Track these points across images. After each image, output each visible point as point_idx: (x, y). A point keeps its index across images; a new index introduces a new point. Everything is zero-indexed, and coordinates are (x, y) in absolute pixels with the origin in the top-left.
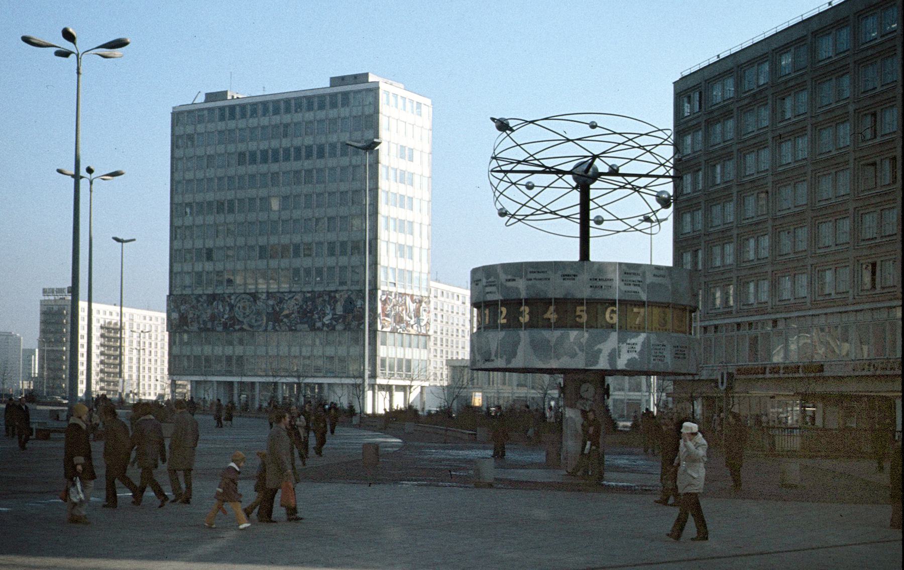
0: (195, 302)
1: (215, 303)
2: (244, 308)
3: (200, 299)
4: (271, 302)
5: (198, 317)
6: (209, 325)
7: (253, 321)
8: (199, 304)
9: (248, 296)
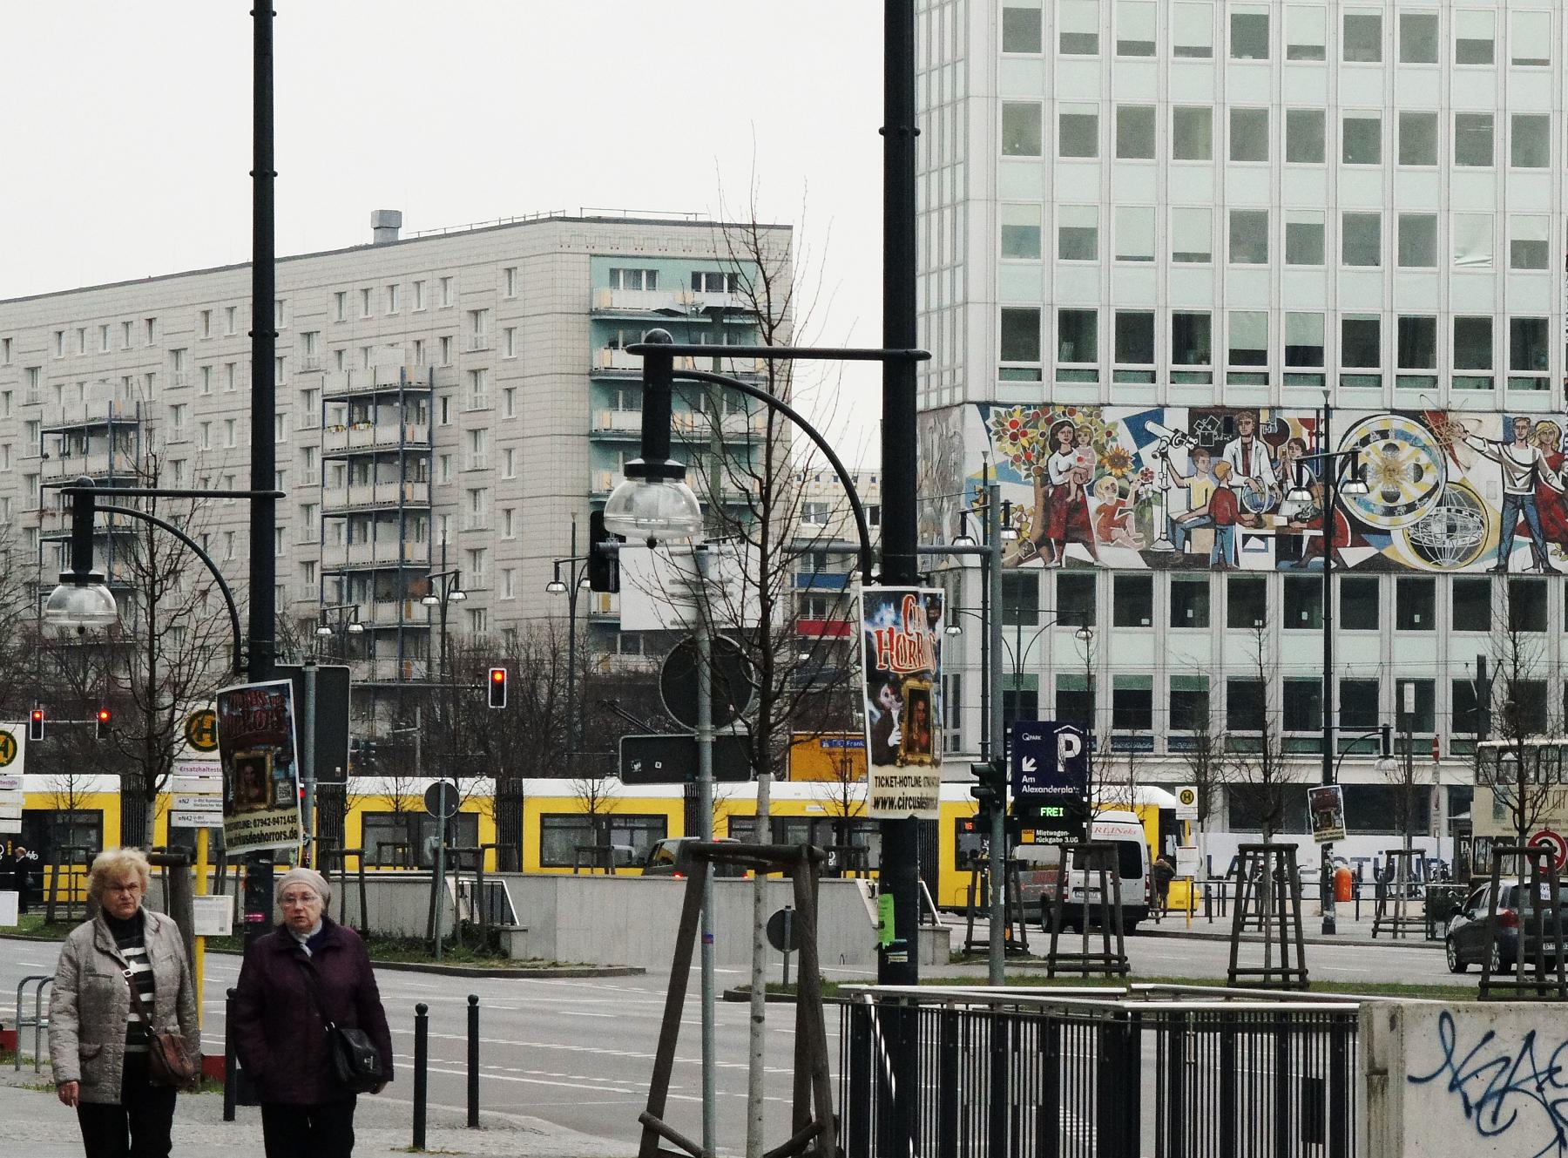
0: (1125, 441)
1: (1233, 448)
2: (1390, 471)
3: (1150, 426)
4: (1523, 454)
5: (1143, 504)
6: (1203, 542)
7: (1438, 529)
8: (1146, 452)
9: (1416, 429)
